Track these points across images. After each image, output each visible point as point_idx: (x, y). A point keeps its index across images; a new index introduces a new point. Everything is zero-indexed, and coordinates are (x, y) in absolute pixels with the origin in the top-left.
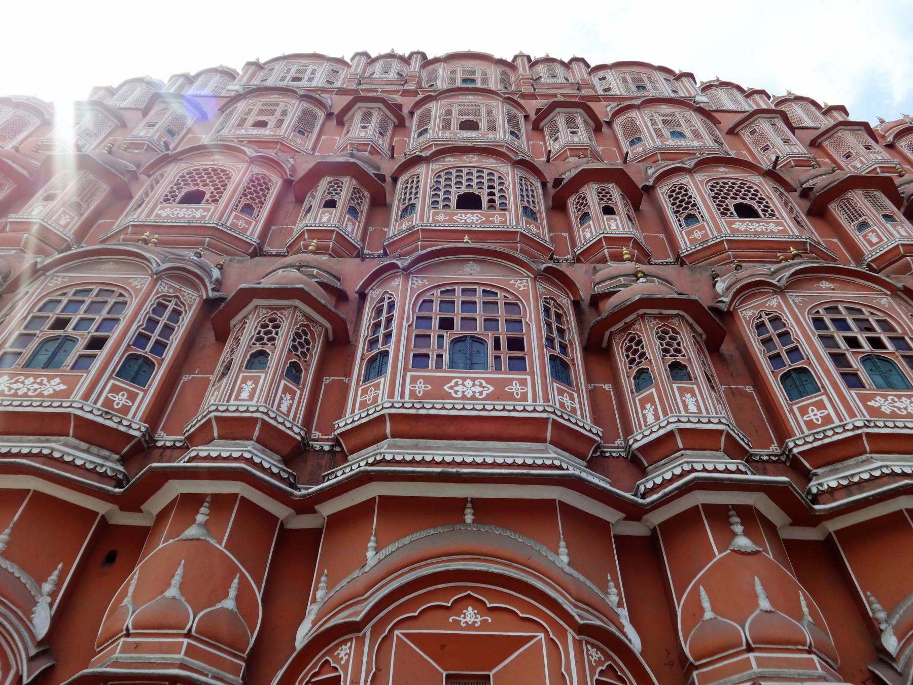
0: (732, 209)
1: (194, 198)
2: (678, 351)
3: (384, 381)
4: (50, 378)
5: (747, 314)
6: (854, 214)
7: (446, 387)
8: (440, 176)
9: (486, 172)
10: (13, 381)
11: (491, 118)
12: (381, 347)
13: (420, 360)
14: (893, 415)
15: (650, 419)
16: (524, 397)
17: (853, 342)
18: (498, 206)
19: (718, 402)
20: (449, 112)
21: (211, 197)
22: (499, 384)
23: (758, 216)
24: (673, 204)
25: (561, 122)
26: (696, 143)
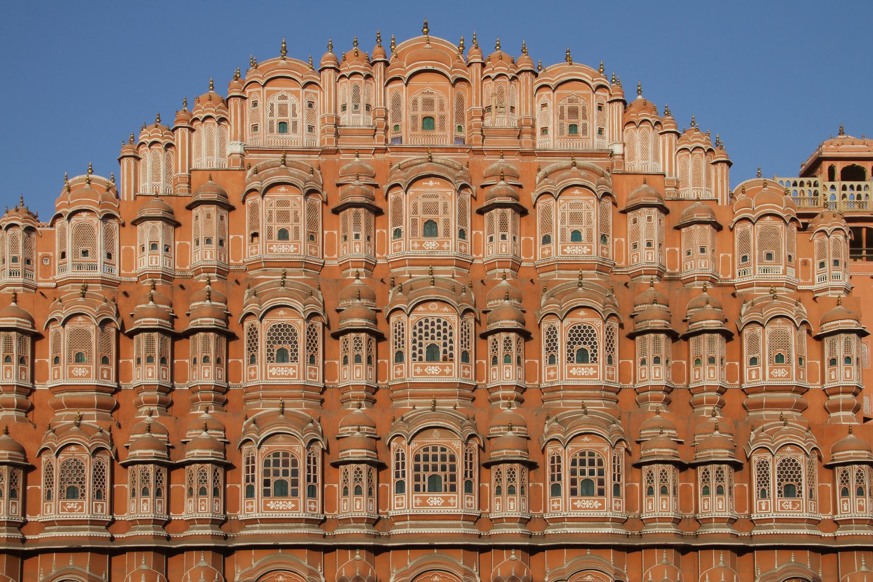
0: (575, 354)
1: (282, 356)
2: (514, 479)
3: (404, 496)
4: (288, 501)
5: (549, 450)
6: (644, 352)
8: (415, 328)
9: (443, 321)
11: (446, 217)
12: (401, 478)
13: (417, 489)
14: (580, 508)
16: (454, 505)
17: (583, 473)
18: (449, 358)
19: (524, 500)
20: (415, 212)
21: (293, 354)
22: (446, 499)
23: (587, 362)
24: (547, 341)
25: (497, 220)
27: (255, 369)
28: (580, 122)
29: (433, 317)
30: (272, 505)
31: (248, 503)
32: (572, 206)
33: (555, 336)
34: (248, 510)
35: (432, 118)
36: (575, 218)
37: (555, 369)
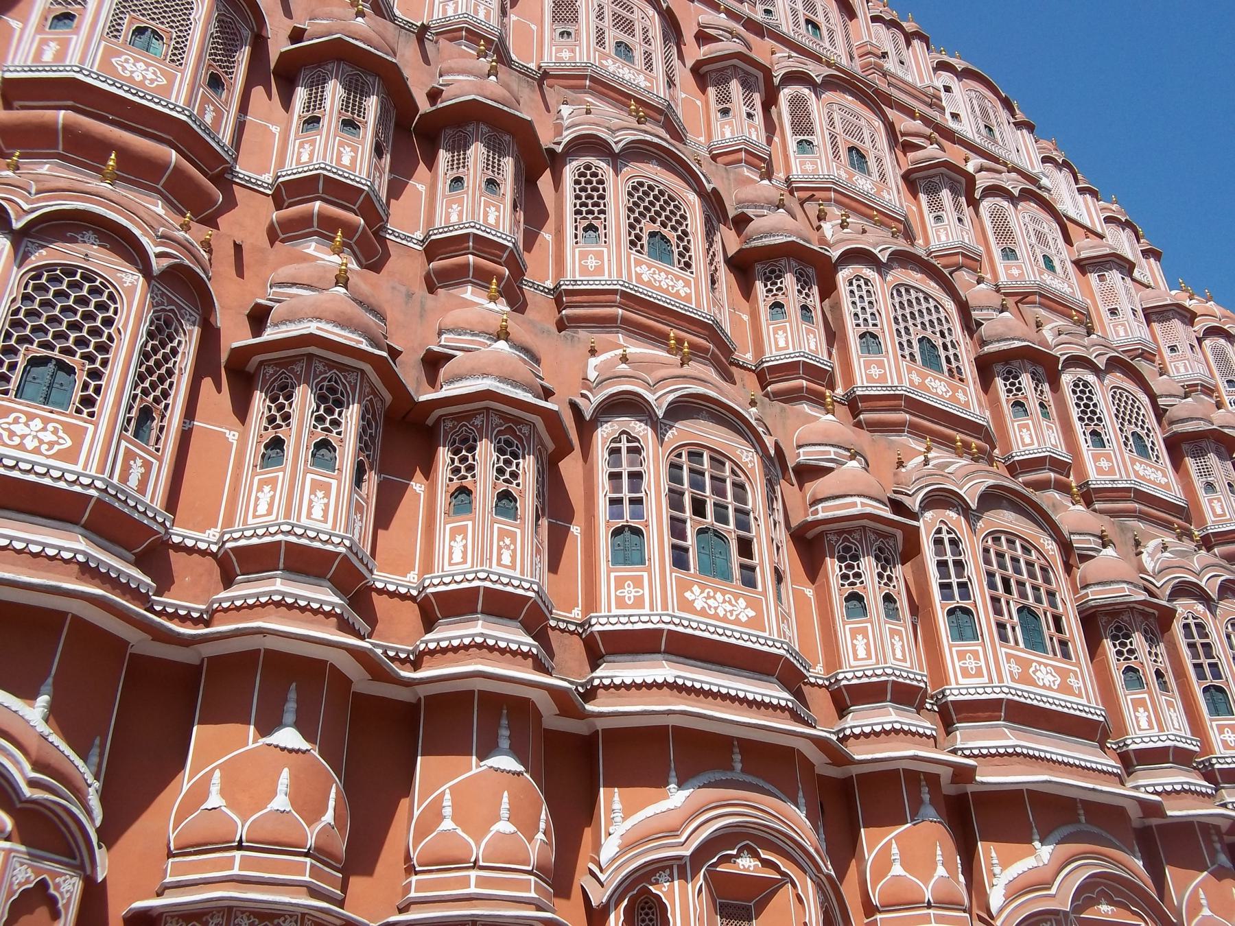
6: (1205, 471)
7: (1031, 671)
9: (932, 303)
10: (705, 595)
12: (957, 602)
15: (1144, 724)
20: (832, 124)
21: (680, 254)
24: (1078, 405)
26: (1069, 290)
27: (599, 256)
28: (995, 129)
29: (918, 290)
30: (697, 596)
31: (620, 583)
32: (1033, 219)
33: (1090, 399)
34: (621, 603)
35: (816, 26)
36: (1040, 236)
37: (1109, 459)
